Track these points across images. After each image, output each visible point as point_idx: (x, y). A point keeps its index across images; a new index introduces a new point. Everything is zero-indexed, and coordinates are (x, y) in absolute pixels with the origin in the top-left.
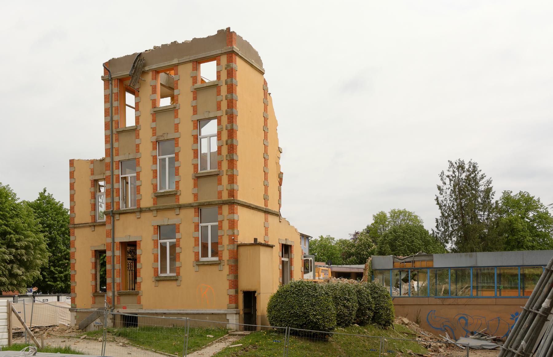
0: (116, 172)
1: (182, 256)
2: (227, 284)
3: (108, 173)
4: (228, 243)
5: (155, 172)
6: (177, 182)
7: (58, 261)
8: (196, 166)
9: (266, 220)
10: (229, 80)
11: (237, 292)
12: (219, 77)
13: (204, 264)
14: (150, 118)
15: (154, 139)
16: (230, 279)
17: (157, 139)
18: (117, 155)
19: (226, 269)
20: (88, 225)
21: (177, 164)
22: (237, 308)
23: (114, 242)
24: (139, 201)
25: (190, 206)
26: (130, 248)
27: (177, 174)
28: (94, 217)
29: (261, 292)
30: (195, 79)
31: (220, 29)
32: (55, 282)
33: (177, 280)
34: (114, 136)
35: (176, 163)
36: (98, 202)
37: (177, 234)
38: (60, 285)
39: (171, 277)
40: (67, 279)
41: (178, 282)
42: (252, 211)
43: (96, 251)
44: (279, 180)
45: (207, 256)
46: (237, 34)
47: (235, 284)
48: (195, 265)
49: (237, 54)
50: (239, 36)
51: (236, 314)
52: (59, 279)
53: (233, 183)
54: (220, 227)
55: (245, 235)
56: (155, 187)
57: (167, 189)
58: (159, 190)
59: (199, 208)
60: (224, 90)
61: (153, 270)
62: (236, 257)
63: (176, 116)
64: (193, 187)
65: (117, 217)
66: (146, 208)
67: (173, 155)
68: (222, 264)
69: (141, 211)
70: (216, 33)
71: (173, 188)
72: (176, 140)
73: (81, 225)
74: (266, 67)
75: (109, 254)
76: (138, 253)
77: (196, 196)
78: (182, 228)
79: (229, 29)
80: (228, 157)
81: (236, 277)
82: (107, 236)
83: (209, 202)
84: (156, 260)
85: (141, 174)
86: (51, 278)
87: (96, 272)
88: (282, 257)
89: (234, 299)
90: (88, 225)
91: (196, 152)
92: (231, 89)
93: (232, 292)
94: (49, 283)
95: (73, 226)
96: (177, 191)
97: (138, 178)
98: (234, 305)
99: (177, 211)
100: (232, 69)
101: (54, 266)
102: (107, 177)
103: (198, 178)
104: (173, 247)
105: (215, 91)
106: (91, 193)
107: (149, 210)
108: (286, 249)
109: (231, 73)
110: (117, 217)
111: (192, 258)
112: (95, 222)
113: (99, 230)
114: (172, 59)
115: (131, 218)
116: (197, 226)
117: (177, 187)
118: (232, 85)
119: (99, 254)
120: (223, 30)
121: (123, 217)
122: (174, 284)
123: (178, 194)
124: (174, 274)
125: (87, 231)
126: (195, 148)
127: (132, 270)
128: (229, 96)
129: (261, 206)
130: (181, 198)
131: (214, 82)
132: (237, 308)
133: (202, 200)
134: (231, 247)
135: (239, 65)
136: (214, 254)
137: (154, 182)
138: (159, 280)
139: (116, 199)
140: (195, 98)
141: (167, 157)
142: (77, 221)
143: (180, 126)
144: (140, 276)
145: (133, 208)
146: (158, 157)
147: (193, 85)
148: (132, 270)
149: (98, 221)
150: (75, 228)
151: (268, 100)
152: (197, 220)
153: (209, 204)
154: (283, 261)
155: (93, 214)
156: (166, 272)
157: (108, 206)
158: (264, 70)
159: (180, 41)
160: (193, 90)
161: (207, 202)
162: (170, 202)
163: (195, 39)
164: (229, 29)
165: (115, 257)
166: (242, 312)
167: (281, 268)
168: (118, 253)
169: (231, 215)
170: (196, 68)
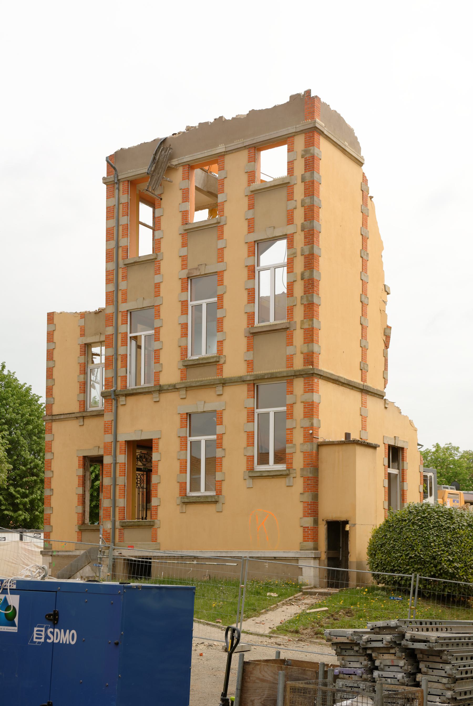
1: (225, 462)
2: (299, 509)
3: (110, 330)
5: (184, 326)
6: (220, 343)
7: (22, 478)
8: (251, 316)
10: (308, 174)
11: (316, 522)
12: (291, 170)
14: (179, 240)
15: (184, 274)
18: (125, 301)
19: (299, 484)
20: (73, 415)
21: (220, 314)
22: (316, 548)
23: (116, 441)
24: (157, 374)
25: (240, 381)
26: (142, 451)
27: (220, 329)
28: (83, 403)
29: (357, 522)
30: (252, 176)
31: (294, 93)
32: (15, 511)
33: (216, 502)
34: (120, 271)
35: (219, 311)
37: (218, 427)
38: (23, 515)
39: (207, 497)
40: (32, 507)
41: (219, 506)
42: (341, 389)
43: (84, 457)
45: (267, 462)
46: (322, 100)
47: (313, 508)
48: (247, 477)
49: (321, 133)
50: (325, 104)
51: (315, 558)
52: (21, 507)
54: (289, 415)
56: (184, 351)
57: (204, 354)
59: (254, 383)
60: (299, 191)
62: (313, 463)
63: (220, 237)
64: (246, 349)
65: (122, 400)
66: (169, 385)
67: (215, 300)
68: (292, 476)
70: (288, 100)
71: (214, 351)
72: (219, 275)
73: (62, 417)
74: (365, 153)
75: (107, 460)
76: (154, 459)
77: (250, 364)
78: (226, 417)
79: (308, 92)
81: (316, 497)
82: (106, 432)
83: (272, 374)
84: (183, 470)
85: (162, 331)
86: (9, 504)
87: (84, 491)
88: (389, 467)
89: (311, 534)
90: (73, 415)
91: (251, 294)
92: (311, 188)
93: (309, 522)
94: (6, 512)
95: (50, 417)
96: (219, 357)
97: (157, 337)
98: (310, 544)
99: (219, 389)
100: (313, 157)
101: (15, 486)
102: (107, 337)
103: (254, 335)
105: (284, 193)
107: (174, 388)
108: (395, 453)
109: (311, 163)
111: (242, 466)
112: (84, 411)
114: (216, 145)
115: (145, 402)
116: (251, 414)
117: (220, 351)
118: (313, 182)
119: (92, 462)
120: (298, 95)
121: (131, 400)
122: (211, 508)
124: (213, 493)
125: (73, 425)
126: (250, 286)
127: (143, 488)
128: (308, 200)
129: (355, 380)
130: (225, 367)
131: (283, 179)
132: (316, 548)
133: (259, 371)
134: (307, 447)
135: (324, 150)
136: (279, 458)
137: (183, 344)
138: (187, 502)
139: (121, 372)
140: (251, 206)
141: (204, 302)
142: (56, 410)
143: (226, 252)
144: (156, 496)
145: (147, 385)
146: (190, 304)
147: (249, 185)
148: (143, 488)
149: (90, 409)
150: (53, 420)
151: (369, 207)
152: (251, 403)
153: (273, 377)
154: (389, 474)
155: (81, 398)
156: (199, 490)
157: (108, 383)
158: (362, 157)
159: (228, 117)
160: (249, 194)
161: (268, 374)
162: (208, 375)
163: (253, 113)
164: (308, 92)
165: (118, 466)
166: (324, 557)
167: (387, 485)
168: (122, 458)
169: (307, 396)
170: (254, 159)
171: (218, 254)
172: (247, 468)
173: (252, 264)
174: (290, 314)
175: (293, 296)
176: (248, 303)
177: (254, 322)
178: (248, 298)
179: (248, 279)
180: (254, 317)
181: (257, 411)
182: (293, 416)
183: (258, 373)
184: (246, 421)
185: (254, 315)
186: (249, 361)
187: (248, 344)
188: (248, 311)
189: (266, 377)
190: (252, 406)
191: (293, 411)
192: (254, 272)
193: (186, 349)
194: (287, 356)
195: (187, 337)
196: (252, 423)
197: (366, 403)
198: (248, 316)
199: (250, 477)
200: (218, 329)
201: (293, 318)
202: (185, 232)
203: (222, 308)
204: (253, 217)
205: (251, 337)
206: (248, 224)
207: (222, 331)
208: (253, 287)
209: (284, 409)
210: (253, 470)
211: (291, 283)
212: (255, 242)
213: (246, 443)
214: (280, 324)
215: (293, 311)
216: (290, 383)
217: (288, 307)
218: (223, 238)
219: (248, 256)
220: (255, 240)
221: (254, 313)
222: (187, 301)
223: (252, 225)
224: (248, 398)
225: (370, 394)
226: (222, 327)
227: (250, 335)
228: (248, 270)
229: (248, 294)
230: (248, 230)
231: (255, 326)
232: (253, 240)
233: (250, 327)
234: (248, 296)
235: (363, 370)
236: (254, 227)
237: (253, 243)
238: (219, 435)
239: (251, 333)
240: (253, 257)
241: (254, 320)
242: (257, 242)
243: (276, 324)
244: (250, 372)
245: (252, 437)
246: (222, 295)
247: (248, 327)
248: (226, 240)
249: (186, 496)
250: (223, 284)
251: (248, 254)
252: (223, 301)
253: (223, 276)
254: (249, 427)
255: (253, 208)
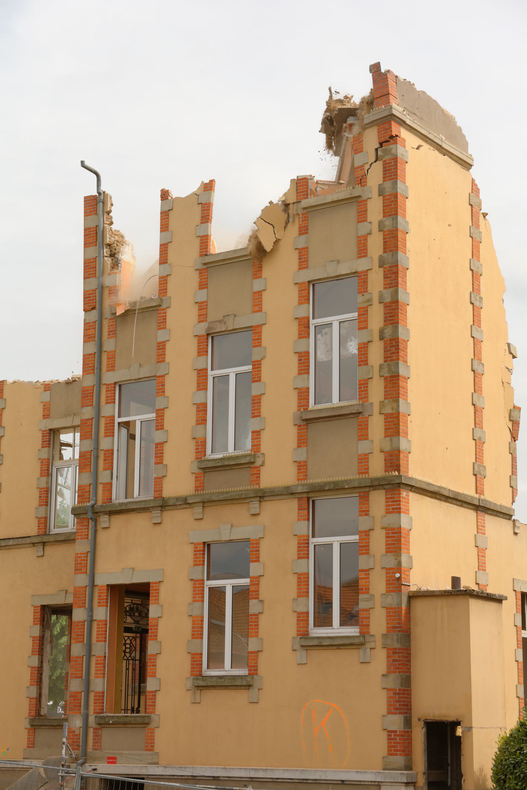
0: (107, 410)
1: (263, 621)
2: (379, 702)
5: (202, 408)
6: (257, 434)
8: (303, 394)
9: (480, 529)
10: (388, 185)
11: (408, 722)
13: (322, 645)
14: (194, 279)
15: (202, 329)
16: (391, 686)
17: (209, 328)
18: (112, 368)
19: (379, 660)
20: (28, 541)
21: (256, 389)
22: (409, 767)
24: (159, 481)
25: (287, 493)
26: (133, 600)
27: (256, 413)
28: (44, 522)
29: (474, 725)
33: (249, 686)
36: (57, 484)
39: (234, 677)
41: (253, 692)
43: (43, 607)
44: (510, 425)
45: (329, 623)
47: (402, 700)
48: (297, 646)
51: (407, 784)
53: (398, 433)
54: (363, 547)
58: (209, 455)
59: (308, 497)
61: (188, 658)
64: (295, 445)
65: (104, 520)
66: (177, 499)
67: (248, 368)
68: (368, 646)
69: (164, 505)
72: (255, 331)
73: (11, 542)
76: (151, 615)
77: (302, 467)
80: (386, 369)
81: (407, 681)
84: (197, 634)
85: (168, 414)
89: (399, 743)
90: (28, 541)
93: (396, 722)
96: (254, 456)
98: (399, 760)
99: (254, 506)
100: (395, 159)
103: (308, 423)
104: (242, 596)
105: (352, 211)
106: (42, 461)
107: (184, 503)
110: (104, 520)
111: (290, 629)
112: (45, 534)
113: (55, 553)
115: (140, 523)
117: (256, 447)
118: (396, 196)
121: (118, 521)
122: (240, 697)
123: (258, 463)
124: (243, 672)
127: (134, 659)
128: (388, 222)
130: (264, 472)
132: (409, 767)
133: (317, 478)
136: (349, 617)
137: (199, 435)
138: (203, 685)
141: (232, 372)
145: (142, 498)
146: (211, 374)
148: (134, 659)
153: (337, 488)
161: (329, 483)
165: (95, 624)
168: (102, 613)
169: (391, 519)
171: (254, 299)
172: (298, 631)
173: (305, 315)
174: (363, 391)
175: (367, 364)
176: (299, 374)
177: (308, 402)
178: (299, 367)
179: (299, 338)
180: (308, 396)
181: (313, 541)
182: (369, 549)
183: (314, 481)
184: (297, 558)
185: (308, 392)
186: (300, 462)
187: (298, 437)
188: (298, 387)
189: (327, 488)
190: (305, 532)
191: (369, 542)
192: (309, 327)
193: (204, 443)
194: (359, 455)
195: (206, 424)
196: (306, 560)
197: (484, 527)
198: (299, 393)
199: (302, 646)
200: (252, 413)
201: (367, 397)
202: (205, 267)
203: (260, 381)
204: (306, 246)
205: (304, 425)
206: (299, 256)
207: (259, 416)
208: (306, 350)
209: (355, 538)
210: (308, 634)
211: (364, 344)
212: (309, 282)
213: (296, 591)
214: (348, 406)
215: (367, 387)
216: (364, 498)
217: (359, 381)
218: (261, 277)
219: (299, 304)
220: (309, 280)
221: (308, 389)
222: (207, 369)
223: (305, 258)
224: (299, 520)
225: (490, 512)
226: (260, 409)
227: (303, 423)
228: (299, 325)
229: (299, 360)
230: (299, 265)
231: (309, 409)
232: (307, 281)
233: (302, 410)
234: (299, 364)
236: (307, 261)
237: (307, 284)
238: (254, 577)
239: (303, 420)
240: (306, 305)
241: (308, 399)
242: (312, 283)
243: (342, 407)
244: (301, 480)
245: (305, 581)
246: (260, 361)
247: (299, 410)
248: (265, 279)
249: (201, 675)
250: (261, 345)
251: (299, 300)
252: (260, 371)
253: (261, 332)
254: (301, 566)
255: (307, 233)
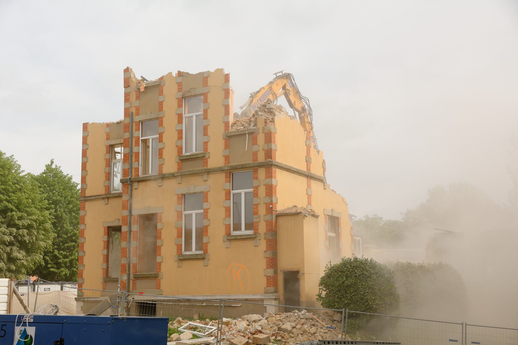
0: (136, 134)
3: (127, 135)
4: (265, 214)
7: (64, 244)
11: (276, 272)
16: (268, 256)
18: (138, 114)
19: (263, 245)
20: (101, 197)
22: (276, 291)
28: (108, 188)
32: (58, 268)
33: (203, 259)
38: (65, 271)
39: (197, 255)
41: (206, 261)
43: (109, 227)
47: (273, 262)
48: (225, 240)
52: (63, 265)
53: (271, 142)
55: (283, 202)
56: (180, 149)
61: (176, 247)
73: (93, 198)
82: (123, 208)
85: (164, 135)
86: (54, 263)
89: (272, 281)
90: (101, 197)
94: (52, 269)
95: (84, 199)
97: (160, 140)
101: (59, 249)
102: (125, 140)
106: (106, 160)
122: (200, 263)
124: (201, 252)
125: (99, 204)
132: (276, 291)
138: (182, 259)
139: (135, 165)
150: (86, 201)
155: (107, 184)
168: (135, 228)
235: (308, 162)
